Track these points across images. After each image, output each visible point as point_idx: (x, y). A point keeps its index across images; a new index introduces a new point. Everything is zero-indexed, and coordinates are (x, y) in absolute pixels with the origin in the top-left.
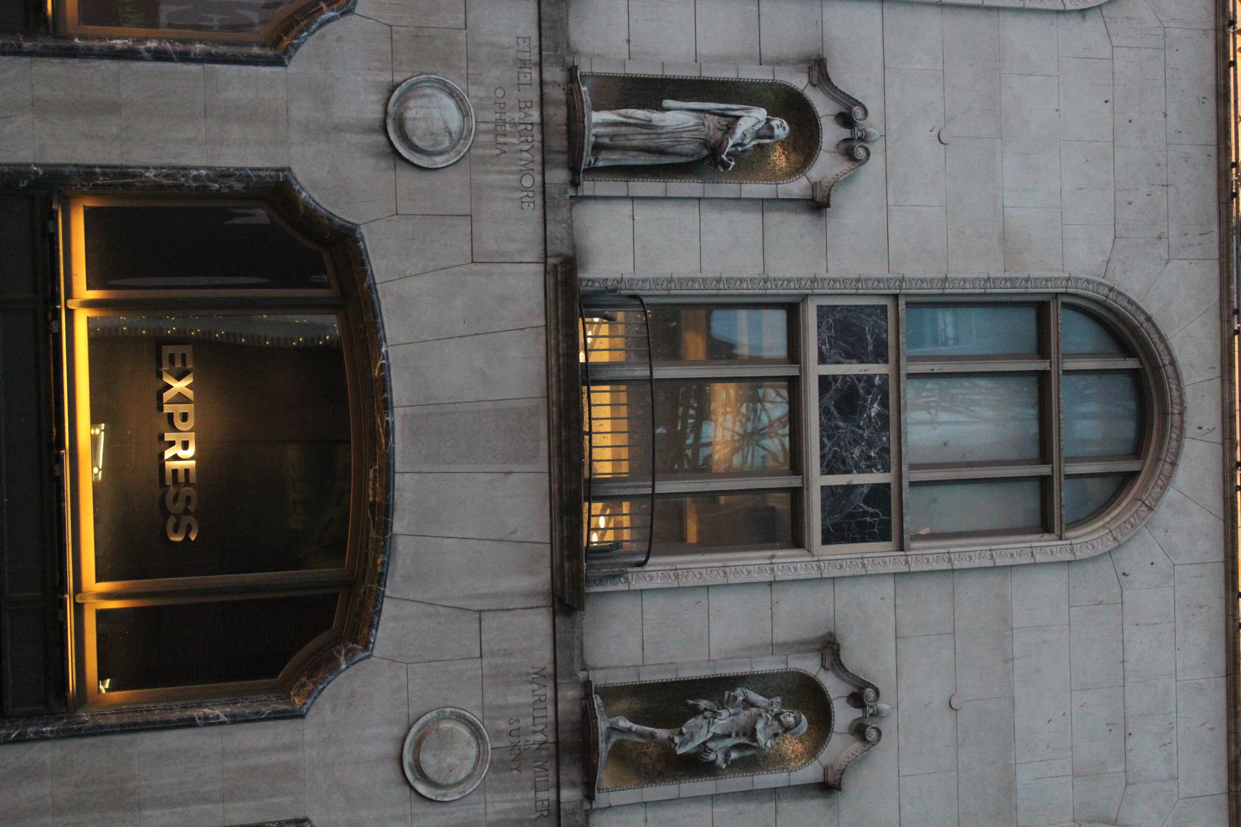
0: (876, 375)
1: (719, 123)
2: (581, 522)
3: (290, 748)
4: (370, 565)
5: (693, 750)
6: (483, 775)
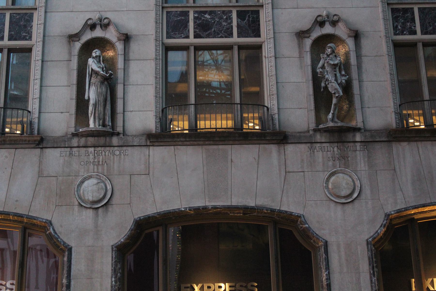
0: (194, 16)
1: (94, 77)
2: (251, 132)
3: (339, 246)
4: (267, 215)
5: (341, 89)
6: (350, 171)
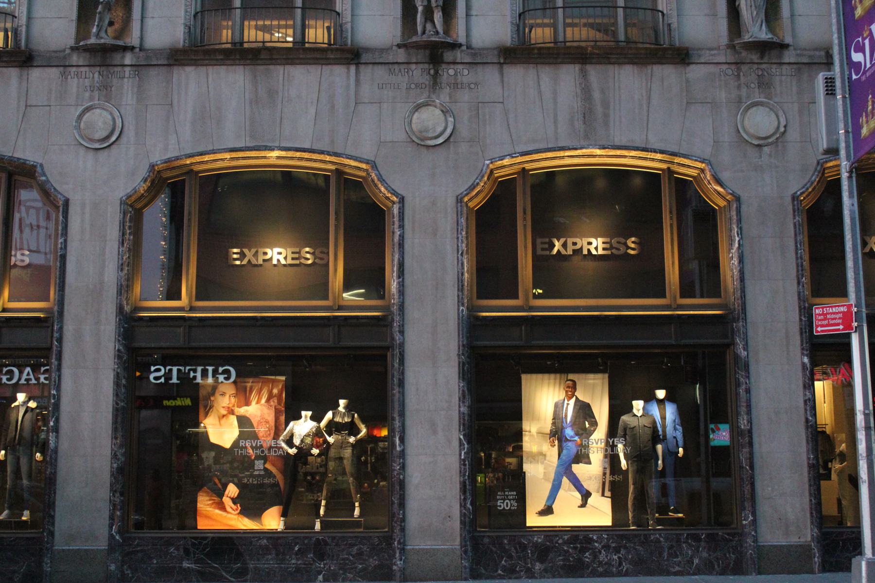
3: (83, 206)
